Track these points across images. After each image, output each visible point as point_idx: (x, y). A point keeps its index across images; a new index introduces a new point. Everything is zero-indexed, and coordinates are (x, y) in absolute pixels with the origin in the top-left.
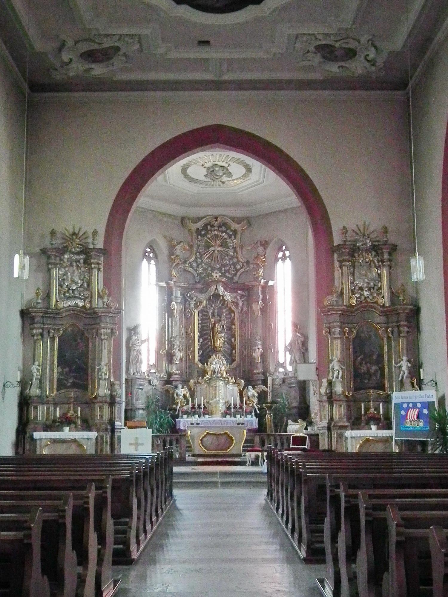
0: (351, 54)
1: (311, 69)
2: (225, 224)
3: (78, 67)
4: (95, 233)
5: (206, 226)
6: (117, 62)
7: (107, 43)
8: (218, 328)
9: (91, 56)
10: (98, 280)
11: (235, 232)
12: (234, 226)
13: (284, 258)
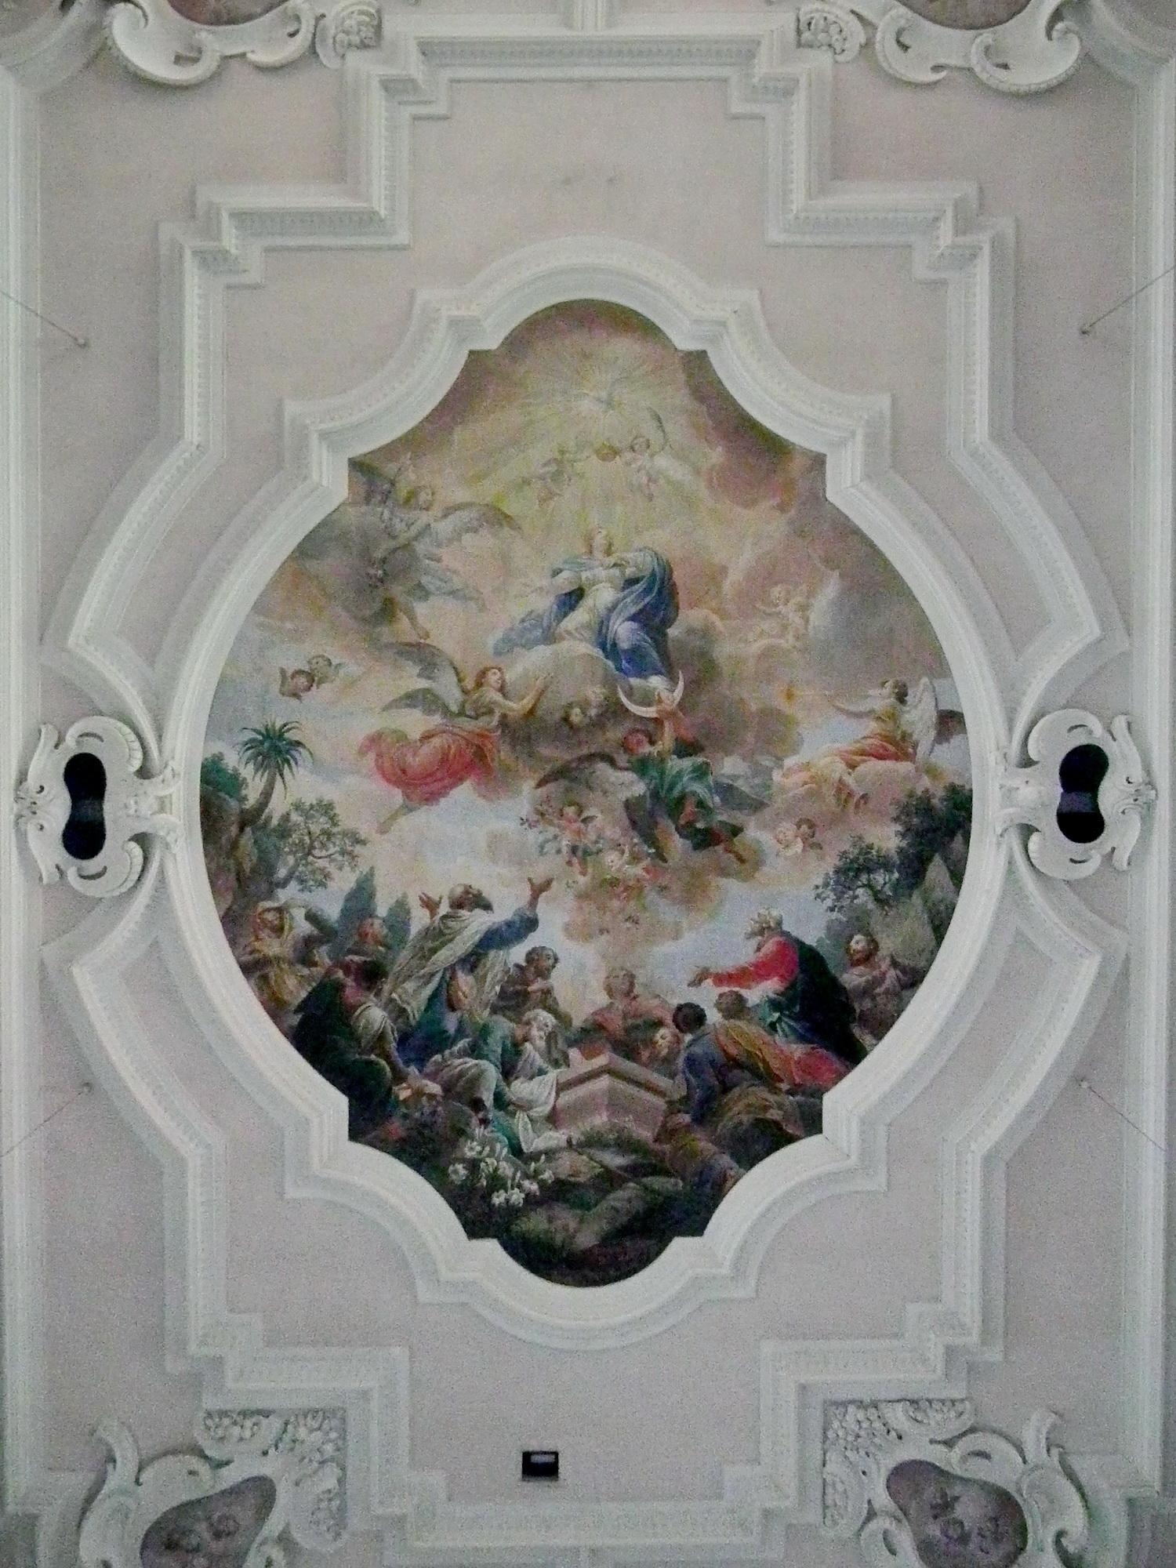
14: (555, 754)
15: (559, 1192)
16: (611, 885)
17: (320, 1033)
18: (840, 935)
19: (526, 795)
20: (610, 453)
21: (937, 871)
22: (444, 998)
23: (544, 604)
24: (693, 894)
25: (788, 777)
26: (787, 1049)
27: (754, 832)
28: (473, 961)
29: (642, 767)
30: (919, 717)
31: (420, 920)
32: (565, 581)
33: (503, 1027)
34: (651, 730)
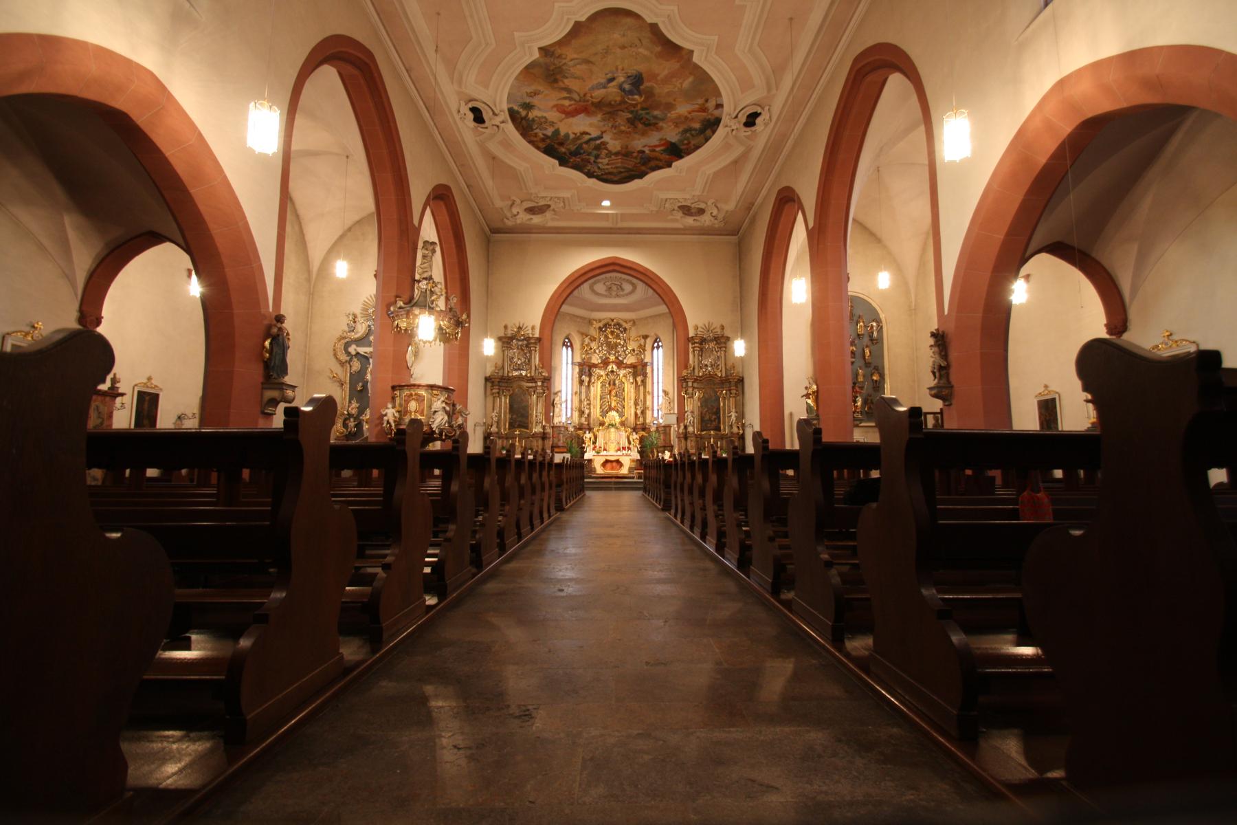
0: (701, 211)
1: (676, 221)
2: (618, 324)
3: (523, 218)
4: (533, 328)
5: (605, 326)
6: (548, 214)
7: (542, 203)
8: (613, 393)
9: (531, 211)
10: (536, 360)
11: (625, 329)
12: (624, 325)
13: (658, 347)
14: (608, 110)
15: (610, 173)
16: (622, 132)
17: (549, 151)
18: (681, 141)
19: (599, 116)
20: (623, 47)
21: (708, 132)
22: (580, 147)
23: (603, 81)
24: (644, 134)
25: (673, 114)
26: (666, 157)
27: (661, 124)
28: (588, 142)
29: (631, 112)
30: (711, 104)
31: (572, 136)
32: (609, 76)
33: (595, 152)
34: (635, 106)
